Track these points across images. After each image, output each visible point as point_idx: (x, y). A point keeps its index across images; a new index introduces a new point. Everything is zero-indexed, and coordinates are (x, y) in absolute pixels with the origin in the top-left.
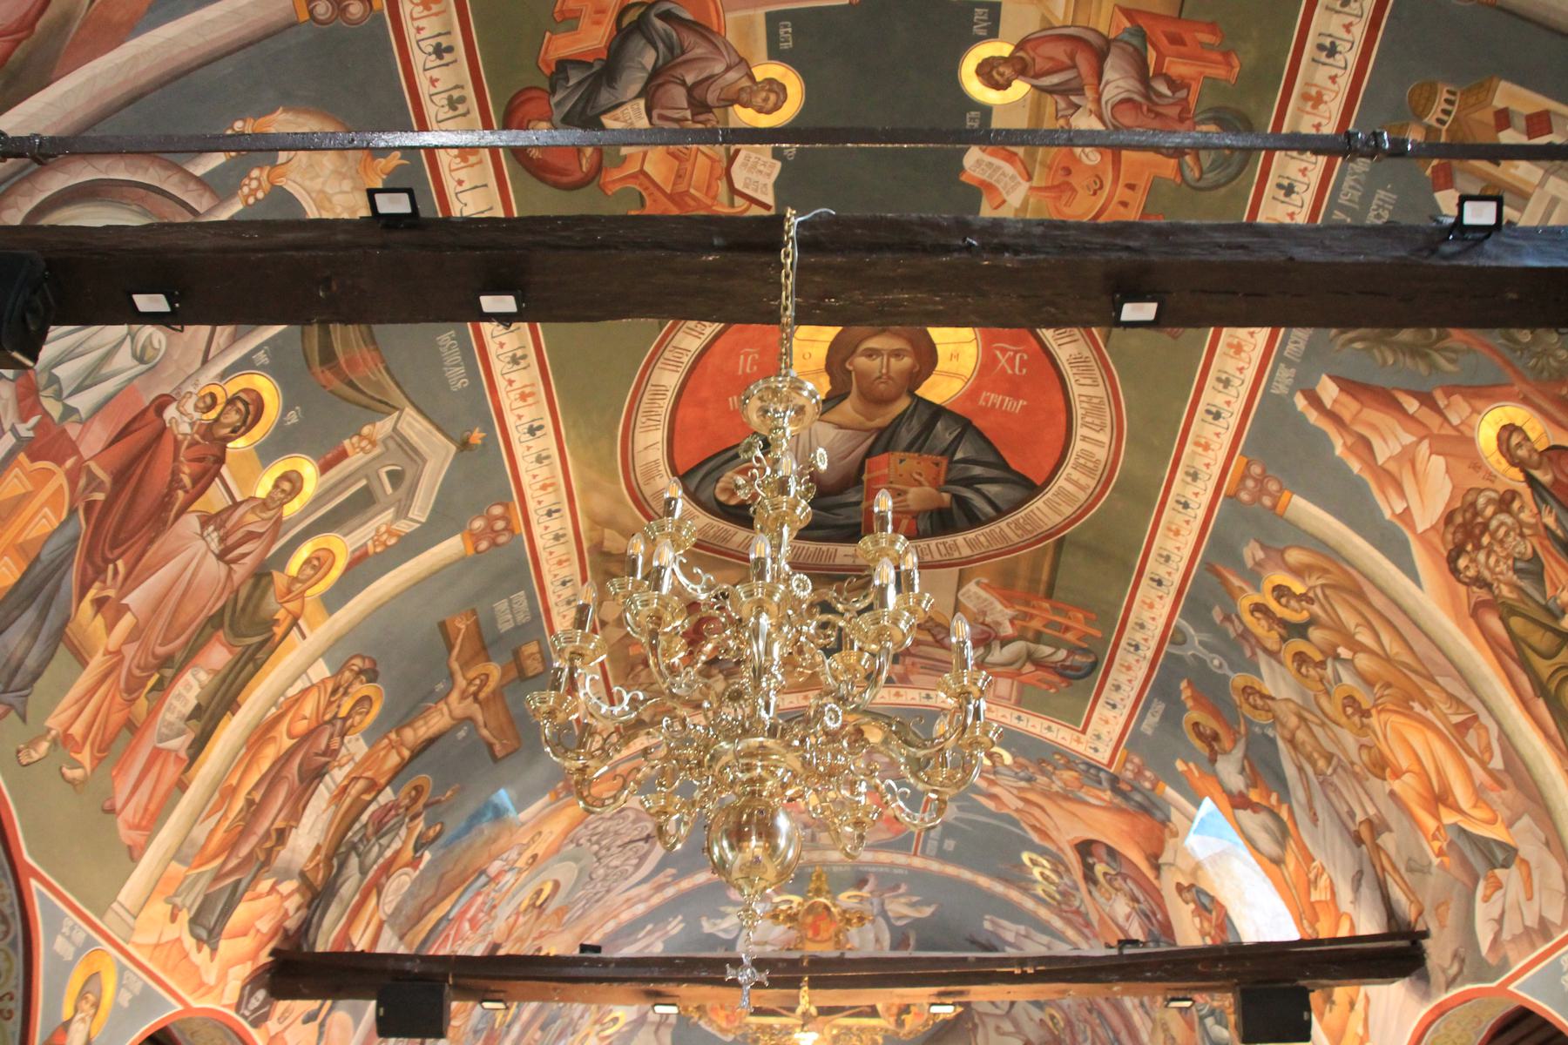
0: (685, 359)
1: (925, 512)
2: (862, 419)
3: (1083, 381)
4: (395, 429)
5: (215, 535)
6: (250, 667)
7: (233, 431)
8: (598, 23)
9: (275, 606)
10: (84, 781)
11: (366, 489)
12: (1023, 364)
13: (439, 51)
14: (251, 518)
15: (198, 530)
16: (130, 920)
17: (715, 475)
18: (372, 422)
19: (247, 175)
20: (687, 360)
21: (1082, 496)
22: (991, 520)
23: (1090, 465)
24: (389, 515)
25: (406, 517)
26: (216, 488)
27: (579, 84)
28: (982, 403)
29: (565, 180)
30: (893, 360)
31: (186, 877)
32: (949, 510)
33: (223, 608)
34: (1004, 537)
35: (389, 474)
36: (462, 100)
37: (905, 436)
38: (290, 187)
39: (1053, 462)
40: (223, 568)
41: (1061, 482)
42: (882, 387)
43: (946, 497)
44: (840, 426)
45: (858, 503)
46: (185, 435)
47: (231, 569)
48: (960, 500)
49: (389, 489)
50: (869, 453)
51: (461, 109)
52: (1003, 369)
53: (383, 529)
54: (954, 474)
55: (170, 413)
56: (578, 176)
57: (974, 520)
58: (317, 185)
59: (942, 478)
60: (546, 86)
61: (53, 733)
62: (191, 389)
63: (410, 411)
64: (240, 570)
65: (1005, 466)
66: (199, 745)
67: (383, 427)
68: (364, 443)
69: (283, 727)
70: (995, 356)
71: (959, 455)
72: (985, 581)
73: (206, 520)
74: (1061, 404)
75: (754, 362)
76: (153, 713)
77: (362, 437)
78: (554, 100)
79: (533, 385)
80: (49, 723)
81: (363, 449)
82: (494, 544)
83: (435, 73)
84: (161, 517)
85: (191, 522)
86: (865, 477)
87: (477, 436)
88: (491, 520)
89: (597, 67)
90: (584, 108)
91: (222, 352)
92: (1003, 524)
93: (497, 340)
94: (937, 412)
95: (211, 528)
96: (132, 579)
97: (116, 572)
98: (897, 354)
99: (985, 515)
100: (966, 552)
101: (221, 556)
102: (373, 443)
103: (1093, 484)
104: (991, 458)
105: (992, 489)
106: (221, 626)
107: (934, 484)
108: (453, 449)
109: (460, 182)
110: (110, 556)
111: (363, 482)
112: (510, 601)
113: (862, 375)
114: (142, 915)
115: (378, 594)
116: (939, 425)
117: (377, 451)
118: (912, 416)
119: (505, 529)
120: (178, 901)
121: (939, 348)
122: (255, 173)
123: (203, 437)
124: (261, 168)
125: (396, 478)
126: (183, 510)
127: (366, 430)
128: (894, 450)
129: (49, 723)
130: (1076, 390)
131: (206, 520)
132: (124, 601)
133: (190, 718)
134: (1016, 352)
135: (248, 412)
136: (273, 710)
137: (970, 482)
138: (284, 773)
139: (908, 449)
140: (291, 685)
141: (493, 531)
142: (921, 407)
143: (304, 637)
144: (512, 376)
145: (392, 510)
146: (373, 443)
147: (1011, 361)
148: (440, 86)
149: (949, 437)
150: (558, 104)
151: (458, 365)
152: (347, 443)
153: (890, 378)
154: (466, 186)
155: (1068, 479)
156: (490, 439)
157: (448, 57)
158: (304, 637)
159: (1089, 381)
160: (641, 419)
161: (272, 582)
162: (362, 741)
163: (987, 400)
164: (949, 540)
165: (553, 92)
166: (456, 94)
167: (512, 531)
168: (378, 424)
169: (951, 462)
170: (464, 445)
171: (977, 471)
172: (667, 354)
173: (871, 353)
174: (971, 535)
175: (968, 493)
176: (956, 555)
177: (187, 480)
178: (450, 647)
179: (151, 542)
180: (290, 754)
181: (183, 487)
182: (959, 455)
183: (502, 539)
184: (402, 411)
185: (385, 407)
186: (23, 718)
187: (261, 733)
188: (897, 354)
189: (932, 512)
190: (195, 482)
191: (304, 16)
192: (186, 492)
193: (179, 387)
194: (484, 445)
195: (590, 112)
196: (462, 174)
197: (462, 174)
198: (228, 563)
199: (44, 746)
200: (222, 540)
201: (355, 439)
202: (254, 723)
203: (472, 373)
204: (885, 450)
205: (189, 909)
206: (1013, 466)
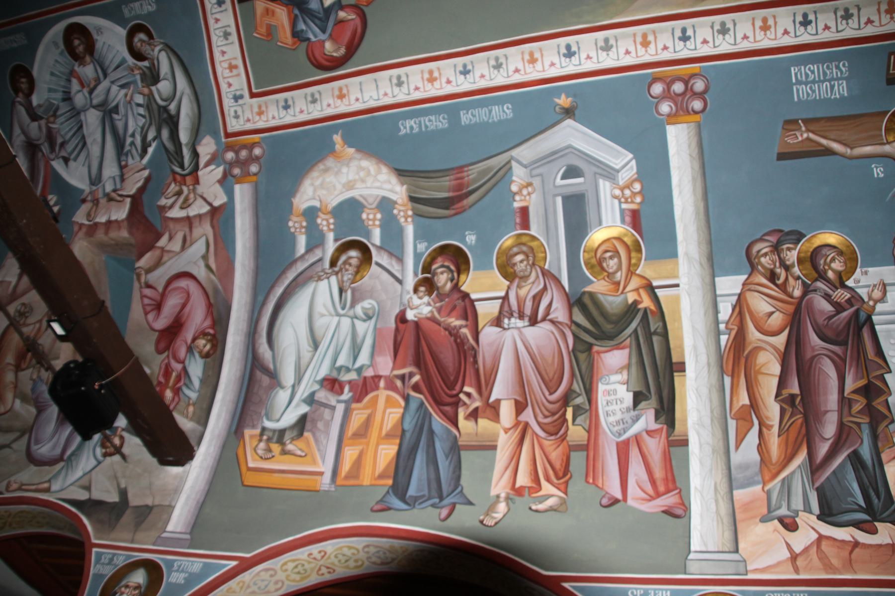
4: (525, 167)
5: (513, 320)
6: (656, 339)
7: (452, 280)
8: (273, 13)
9: (619, 299)
10: (563, 502)
11: (566, 199)
13: (286, 107)
14: (523, 292)
15: (499, 329)
16: (735, 557)
18: (512, 182)
19: (318, 225)
24: (605, 187)
25: (618, 171)
26: (480, 307)
27: (305, 22)
29: (359, 30)
31: (769, 494)
33: (575, 337)
35: (563, 178)
36: (313, 95)
38: (335, 203)
40: (546, 326)
46: (432, 312)
47: (552, 322)
49: (580, 180)
51: (317, 96)
53: (617, 192)
55: (410, 315)
56: (358, 22)
58: (339, 187)
60: (305, 44)
61: (503, 495)
62: (408, 296)
63: (514, 153)
64: (560, 312)
66: (667, 411)
67: (519, 175)
68: (525, 192)
69: (753, 334)
73: (498, 322)
76: (593, 428)
77: (519, 193)
78: (313, 39)
79: (523, 53)
80: (494, 492)
81: (529, 194)
82: (701, 95)
83: (298, 110)
84: (466, 352)
85: (489, 334)
87: (564, 101)
88: (667, 95)
89: (296, 12)
90: (320, 19)
91: (403, 270)
93: (477, 79)
95: (506, 321)
96: (484, 385)
97: (469, 395)
101: (533, 321)
102: (530, 184)
106: (590, 346)
108: (569, 122)
109: (357, 100)
110: (454, 392)
111: (559, 200)
112: (799, 82)
114: (741, 546)
115: (691, 209)
117: (536, 182)
119: (686, 83)
120: (783, 511)
122: (319, 221)
123: (441, 301)
124: (318, 217)
125: (572, 172)
126: (476, 334)
127: (514, 188)
129: (494, 492)
131: (498, 322)
132: (492, 399)
133: (636, 403)
135: (448, 267)
136: (724, 338)
138: (809, 355)
140: (716, 311)
141: (684, 94)
143: (677, 286)
144: (512, 68)
145: (601, 182)
146: (530, 184)
148: (304, 108)
150: (316, 36)
151: (490, 112)
152: (516, 205)
154: (359, 96)
156: (567, 91)
157: (290, 102)
158: (677, 286)
161: (592, 295)
162: (870, 269)
165: (308, 39)
166: (309, 99)
167: (693, 76)
168: (514, 178)
170: (569, 113)
177: (458, 323)
178: (829, 152)
179: (475, 362)
180: (796, 342)
181: (461, 327)
183: (699, 86)
184: (512, 158)
185: (506, 169)
186: (470, 503)
187: (736, 358)
190: (466, 318)
191: (254, 178)
192: (466, 326)
193: (401, 303)
194: (575, 96)
195: (321, 15)
196: (353, 98)
197: (353, 98)
198: (544, 319)
199: (502, 507)
200: (521, 316)
201: (517, 198)
202: (713, 359)
203: (500, 101)
205: (808, 509)
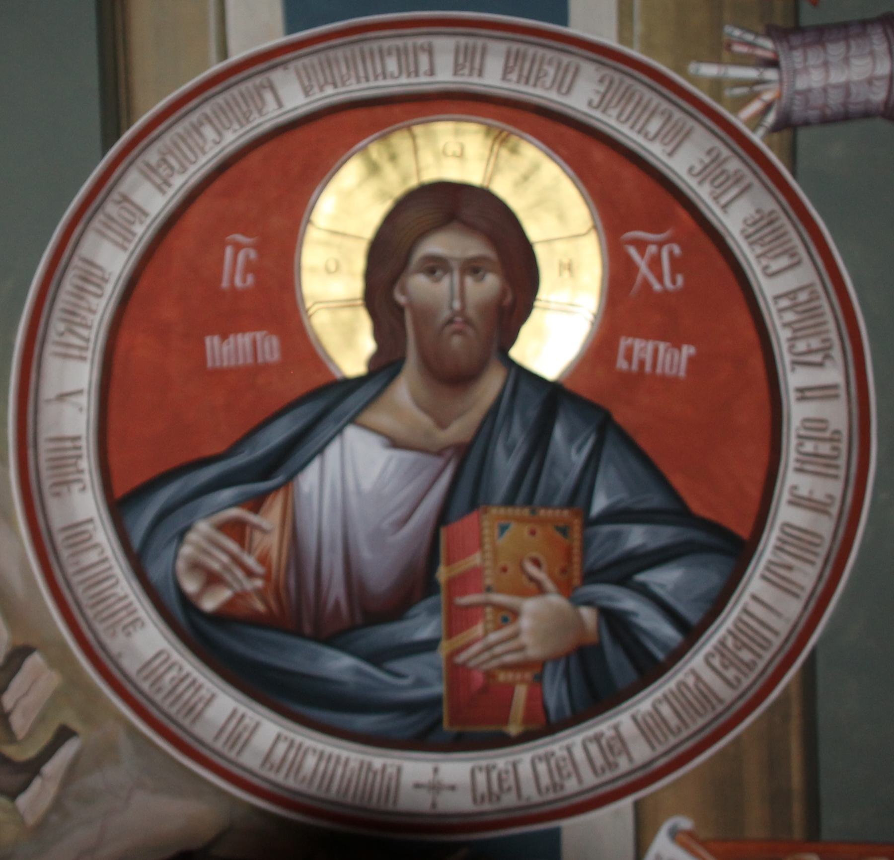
0: (139, 229)
1: (555, 660)
2: (425, 420)
3: (775, 266)
12: (676, 264)
17: (178, 520)
20: (142, 231)
21: (825, 526)
22: (676, 655)
23: (825, 448)
28: (622, 364)
30: (469, 281)
32: (598, 647)
34: (706, 695)
37: (505, 466)
39: (759, 475)
41: (784, 513)
42: (456, 341)
43: (588, 614)
44: (394, 443)
45: (430, 645)
48: (616, 622)
50: (443, 516)
52: (646, 284)
54: (599, 555)
57: (649, 668)
59: (576, 572)
65: (678, 512)
70: (629, 260)
71: (600, 503)
72: (685, 823)
74: (751, 335)
75: (249, 267)
86: (443, 574)
92: (697, 661)
94: (552, 397)
98: (473, 268)
99: (663, 646)
100: (641, 752)
103: (835, 488)
104: (655, 500)
105: (665, 579)
107: (566, 589)
113: (424, 315)
116: (559, 433)
118: (510, 413)
121: (541, 252)
128: (488, 503)
130: (768, 289)
134: (660, 245)
137: (625, 570)
139: (510, 501)
142: (525, 387)
147: (655, 263)
149: (578, 459)
153: (467, 322)
155: (797, 502)
159: (784, 262)
160: (57, 326)
163: (629, 357)
164: (603, 726)
169: (589, 523)
171: (637, 537)
172: (111, 208)
173: (435, 266)
174: (644, 703)
175: (627, 602)
176: (624, 765)
182: (600, 503)
188: (473, 268)
189: (568, 656)
204: (475, 503)
206: (696, 507)
